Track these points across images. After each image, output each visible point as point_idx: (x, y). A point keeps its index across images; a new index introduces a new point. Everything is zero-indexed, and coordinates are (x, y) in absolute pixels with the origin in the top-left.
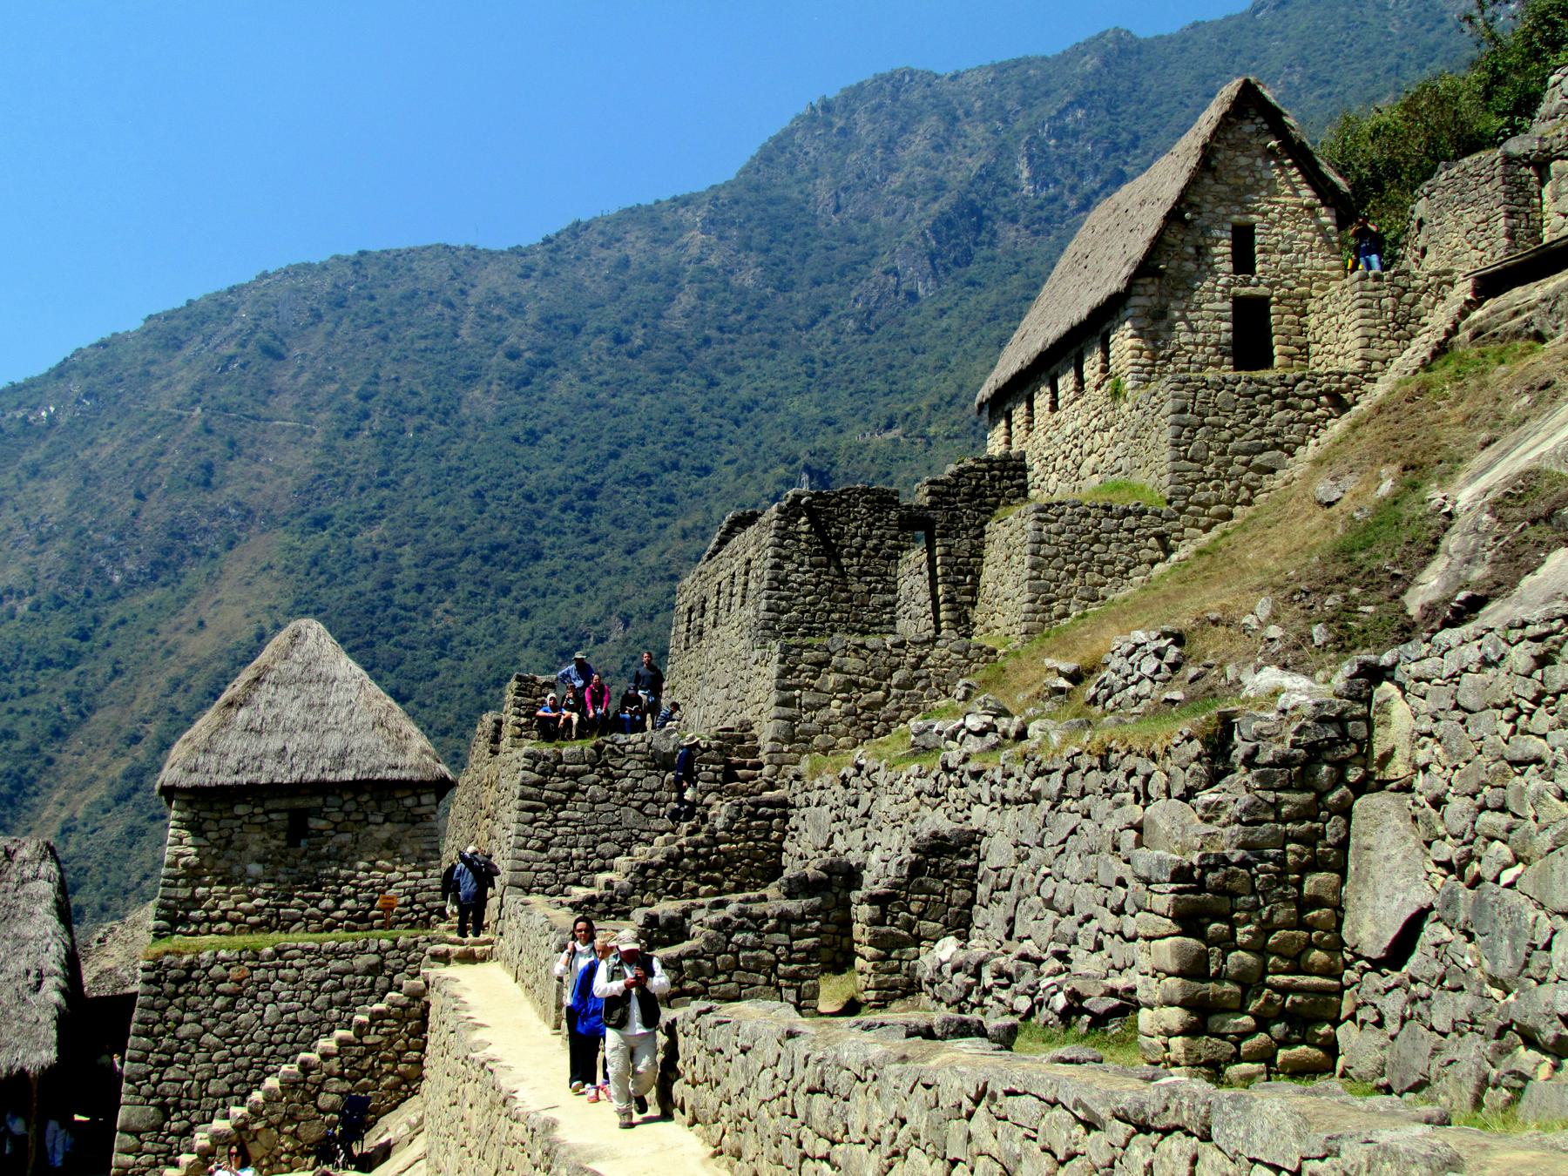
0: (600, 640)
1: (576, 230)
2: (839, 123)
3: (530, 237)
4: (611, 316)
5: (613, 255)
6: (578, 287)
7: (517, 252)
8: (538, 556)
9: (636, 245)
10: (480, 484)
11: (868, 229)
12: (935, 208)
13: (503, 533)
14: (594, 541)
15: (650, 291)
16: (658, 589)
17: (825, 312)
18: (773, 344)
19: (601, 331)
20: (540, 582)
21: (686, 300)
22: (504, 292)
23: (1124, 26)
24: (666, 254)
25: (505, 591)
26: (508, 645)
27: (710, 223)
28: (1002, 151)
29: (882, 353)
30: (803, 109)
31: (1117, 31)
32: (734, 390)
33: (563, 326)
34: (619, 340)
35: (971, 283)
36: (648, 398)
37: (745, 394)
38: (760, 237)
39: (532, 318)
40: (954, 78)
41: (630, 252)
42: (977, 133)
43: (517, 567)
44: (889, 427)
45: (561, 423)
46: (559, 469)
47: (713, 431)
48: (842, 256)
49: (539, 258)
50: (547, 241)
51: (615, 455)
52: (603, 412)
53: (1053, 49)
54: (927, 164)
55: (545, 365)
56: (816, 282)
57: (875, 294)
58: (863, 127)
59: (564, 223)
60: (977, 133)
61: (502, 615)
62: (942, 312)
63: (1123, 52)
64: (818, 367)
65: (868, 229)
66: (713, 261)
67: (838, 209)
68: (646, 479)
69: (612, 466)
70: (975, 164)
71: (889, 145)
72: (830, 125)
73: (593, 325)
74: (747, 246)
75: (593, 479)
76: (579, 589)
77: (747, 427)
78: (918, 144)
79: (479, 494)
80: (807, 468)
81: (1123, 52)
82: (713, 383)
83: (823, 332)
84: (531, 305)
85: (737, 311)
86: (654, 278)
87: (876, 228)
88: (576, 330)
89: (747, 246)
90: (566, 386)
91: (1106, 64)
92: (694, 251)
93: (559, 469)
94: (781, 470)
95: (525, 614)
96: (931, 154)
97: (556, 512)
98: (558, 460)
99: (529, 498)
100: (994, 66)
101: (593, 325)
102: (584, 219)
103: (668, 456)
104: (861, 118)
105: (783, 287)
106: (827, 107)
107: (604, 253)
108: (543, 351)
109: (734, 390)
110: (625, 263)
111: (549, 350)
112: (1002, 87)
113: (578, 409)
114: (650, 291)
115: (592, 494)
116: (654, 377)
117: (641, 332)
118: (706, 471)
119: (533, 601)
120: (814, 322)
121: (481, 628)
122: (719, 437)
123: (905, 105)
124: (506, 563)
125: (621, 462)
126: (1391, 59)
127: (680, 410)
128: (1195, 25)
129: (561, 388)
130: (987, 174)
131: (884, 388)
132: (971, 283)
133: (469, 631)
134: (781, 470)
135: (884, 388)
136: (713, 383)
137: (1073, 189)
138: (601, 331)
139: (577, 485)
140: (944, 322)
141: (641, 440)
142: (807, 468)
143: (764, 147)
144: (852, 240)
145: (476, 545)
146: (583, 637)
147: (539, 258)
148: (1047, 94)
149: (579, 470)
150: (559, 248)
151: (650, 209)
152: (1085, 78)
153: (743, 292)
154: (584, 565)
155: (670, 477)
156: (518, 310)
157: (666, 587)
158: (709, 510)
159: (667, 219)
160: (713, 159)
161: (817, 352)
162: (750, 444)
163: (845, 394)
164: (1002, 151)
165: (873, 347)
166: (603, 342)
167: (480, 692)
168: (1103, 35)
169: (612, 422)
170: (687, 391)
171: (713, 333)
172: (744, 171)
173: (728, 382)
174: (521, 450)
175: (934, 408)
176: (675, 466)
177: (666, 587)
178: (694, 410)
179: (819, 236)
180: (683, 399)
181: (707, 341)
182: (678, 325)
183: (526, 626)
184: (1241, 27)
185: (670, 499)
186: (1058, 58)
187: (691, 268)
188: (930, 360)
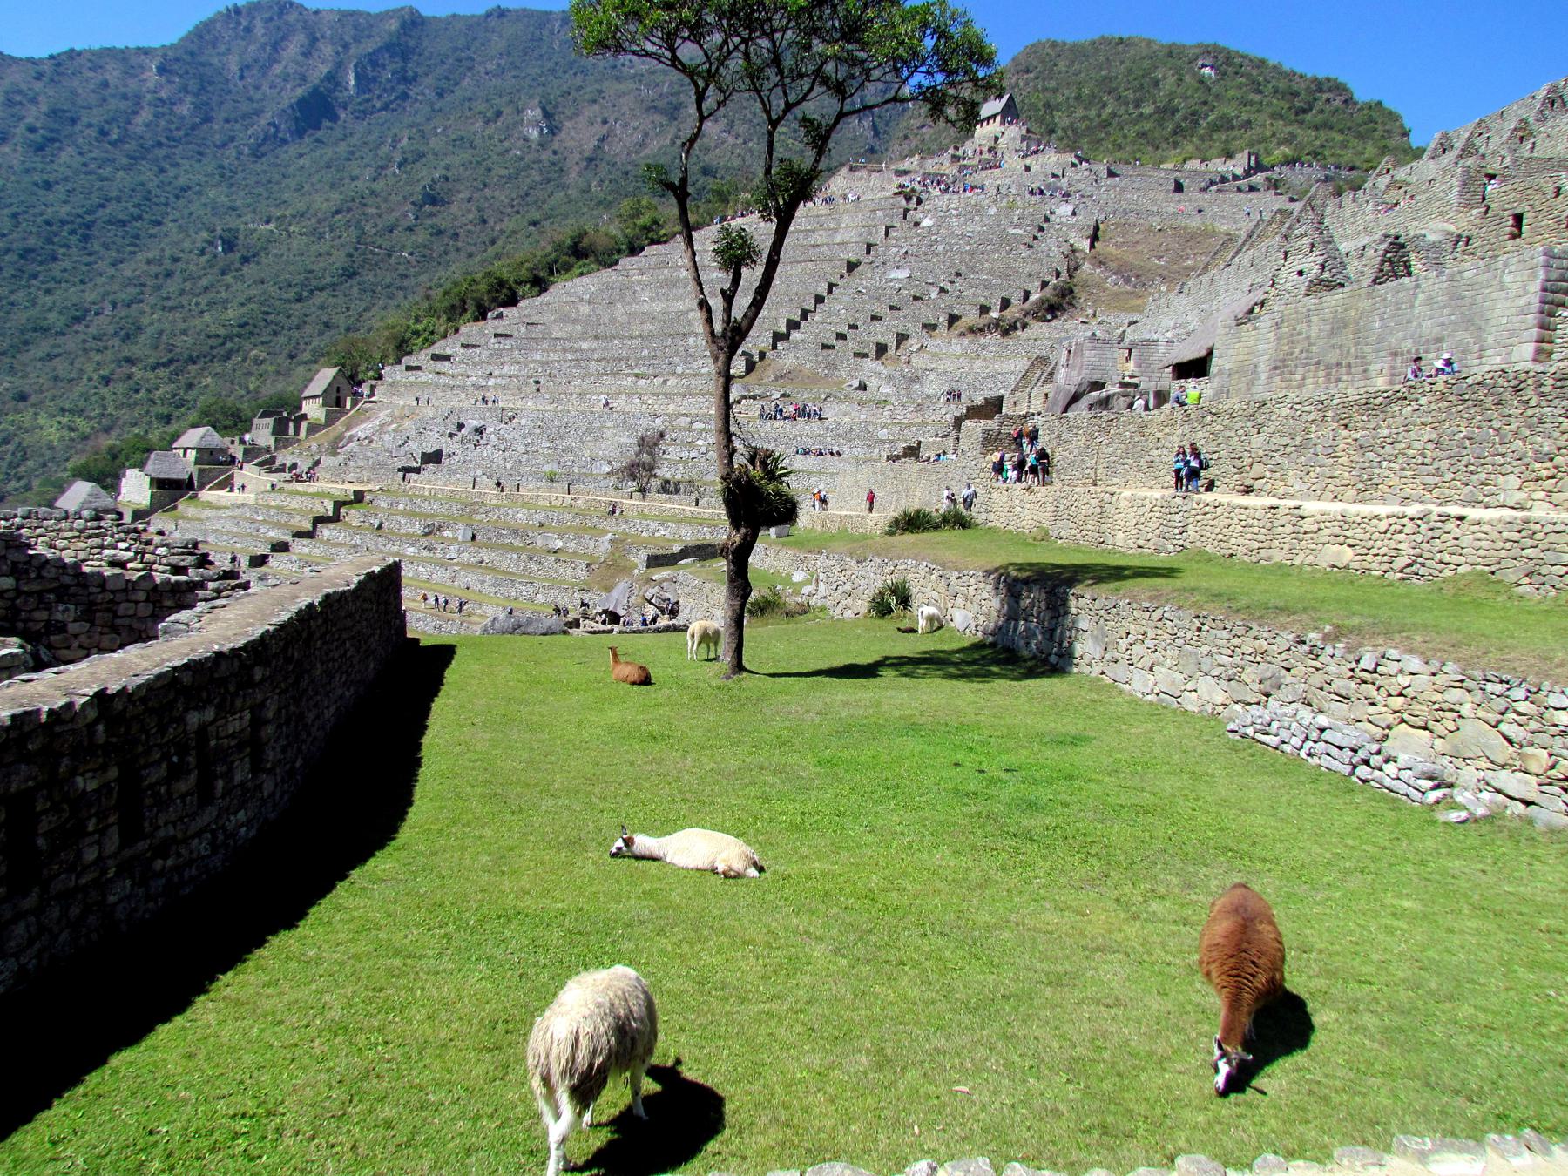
0: (97, 314)
1: (72, 54)
2: (245, 23)
3: (41, 53)
4: (97, 116)
5: (98, 77)
6: (74, 92)
7: (32, 61)
8: (55, 259)
9: (113, 74)
10: (14, 209)
11: (258, 95)
12: (300, 92)
13: (32, 242)
14: (90, 254)
15: (123, 105)
16: (133, 291)
17: (232, 139)
18: (200, 153)
19: (90, 125)
20: (58, 274)
21: (145, 115)
22: (23, 87)
23: (416, 5)
24: (133, 85)
25: (35, 276)
26: (38, 308)
27: (162, 70)
28: (339, 65)
29: (265, 172)
30: (223, 9)
31: (411, 8)
32: (176, 177)
33: (63, 118)
34: (103, 133)
35: (318, 141)
36: (121, 173)
37: (182, 181)
38: (193, 85)
39: (44, 108)
40: (317, 12)
41: (108, 76)
42: (327, 50)
43: (41, 263)
44: (268, 222)
45: (66, 179)
46: (66, 209)
47: (163, 200)
48: (245, 107)
49: (47, 68)
50: (52, 57)
51: (102, 206)
52: (93, 177)
53: (375, 10)
54: (297, 63)
55: (53, 140)
56: (227, 121)
57: (262, 136)
58: (259, 30)
59: (65, 48)
60: (327, 50)
61: (32, 290)
62: (301, 155)
63: (414, 23)
64: (229, 175)
65: (258, 95)
66: (163, 94)
67: (242, 78)
68: (123, 223)
69: (100, 212)
70: (324, 69)
71: (276, 47)
72: (239, 23)
73: (85, 120)
74: (185, 89)
75: (89, 218)
76: (82, 282)
77: (182, 202)
78: (292, 49)
79: (15, 216)
80: (221, 237)
81: (414, 23)
82: (162, 171)
83: (231, 152)
84: (42, 99)
85: (178, 129)
86: (125, 97)
87: (264, 95)
88: (74, 121)
89: (185, 89)
90: (66, 157)
91: (403, 26)
92: (151, 85)
93: (66, 209)
94: (205, 235)
95: (48, 291)
96: (300, 58)
97: (65, 234)
98: (65, 202)
99: (48, 223)
100: (339, 11)
101: (85, 120)
102: (78, 48)
103: (136, 211)
104: (259, 23)
105: (207, 119)
106: (237, 11)
107: (91, 74)
108: (52, 131)
109: (176, 177)
110: (105, 85)
111: (57, 131)
112: (343, 26)
113: (77, 172)
114: (123, 105)
115: (88, 226)
116: (125, 161)
117: (116, 131)
118: (159, 223)
119: (52, 285)
120: (224, 145)
121: (19, 296)
122: (166, 204)
123: (286, 23)
124: (34, 260)
125: (108, 211)
126: (550, 64)
127: (143, 184)
128: (454, 16)
129: (64, 156)
130: (330, 77)
131: (266, 194)
132: (318, 141)
133: (13, 298)
134: (205, 235)
135: (266, 194)
136: (162, 171)
137: (379, 97)
138: (90, 125)
139: (79, 220)
140: (301, 162)
141: (119, 199)
142: (221, 237)
143: (197, 27)
144: (250, 99)
145: (14, 246)
146: (88, 310)
147: (46, 68)
148: (369, 37)
149: (80, 211)
150: (59, 65)
151: (122, 51)
152: (391, 34)
153: (183, 118)
154: (85, 268)
155: (138, 224)
156: (34, 101)
157: (138, 290)
158: (163, 250)
159: (134, 61)
160: (165, 29)
161: (226, 163)
162: (186, 212)
163: (242, 193)
164: (339, 65)
165: (258, 167)
166: (93, 133)
167: (23, 332)
168: (403, 9)
169: (98, 184)
170: (147, 173)
171: (163, 140)
172: (182, 39)
173: (172, 172)
174: (41, 192)
175: (294, 216)
176: (140, 218)
177: (138, 290)
178: (150, 185)
179: (230, 92)
180: (142, 178)
181: (160, 144)
182: (139, 130)
183: (49, 299)
184: (479, 24)
185: (137, 237)
186: (377, 15)
187: (149, 96)
188: (292, 183)
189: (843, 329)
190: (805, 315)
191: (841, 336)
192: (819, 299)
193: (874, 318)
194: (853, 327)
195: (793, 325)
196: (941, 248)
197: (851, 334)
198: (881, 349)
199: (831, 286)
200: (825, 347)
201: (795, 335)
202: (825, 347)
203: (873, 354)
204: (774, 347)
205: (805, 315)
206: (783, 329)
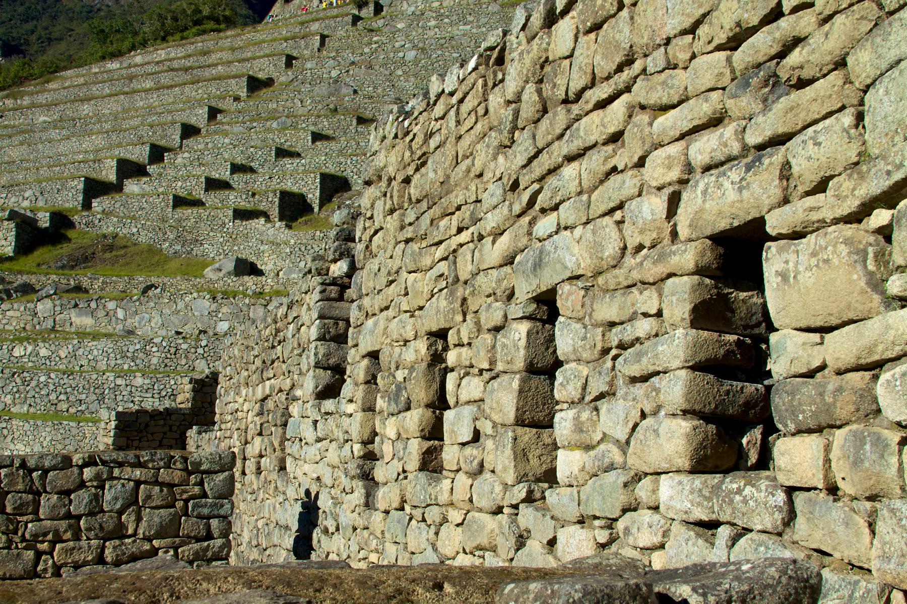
189: (223, 173)
190: (158, 154)
191: (213, 184)
192: (189, 131)
193: (281, 153)
194: (236, 168)
195: (130, 169)
196: (411, 55)
197: (237, 180)
198: (294, 208)
199: (213, 113)
200: (179, 202)
201: (132, 186)
202: (179, 202)
203: (275, 212)
204: (87, 205)
205: (158, 154)
206: (112, 177)
